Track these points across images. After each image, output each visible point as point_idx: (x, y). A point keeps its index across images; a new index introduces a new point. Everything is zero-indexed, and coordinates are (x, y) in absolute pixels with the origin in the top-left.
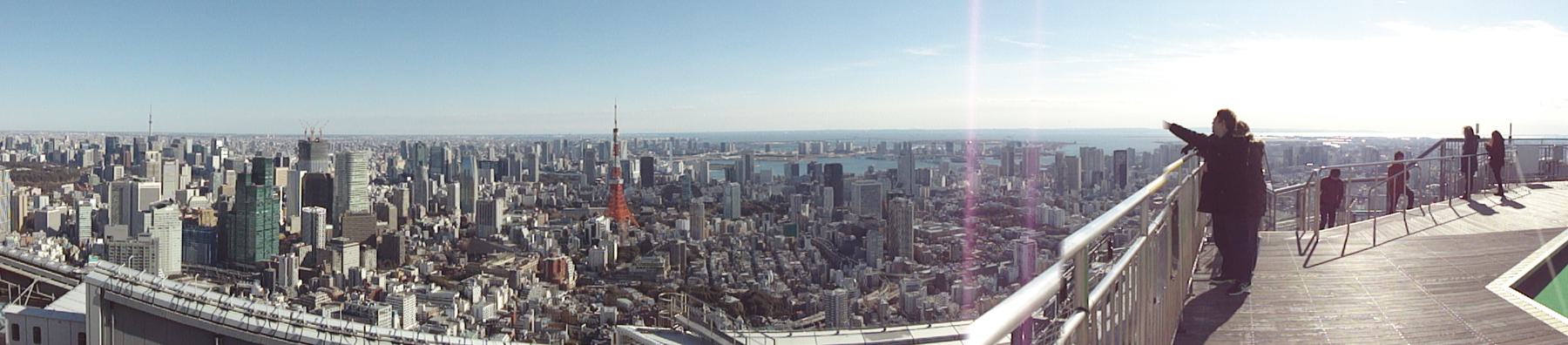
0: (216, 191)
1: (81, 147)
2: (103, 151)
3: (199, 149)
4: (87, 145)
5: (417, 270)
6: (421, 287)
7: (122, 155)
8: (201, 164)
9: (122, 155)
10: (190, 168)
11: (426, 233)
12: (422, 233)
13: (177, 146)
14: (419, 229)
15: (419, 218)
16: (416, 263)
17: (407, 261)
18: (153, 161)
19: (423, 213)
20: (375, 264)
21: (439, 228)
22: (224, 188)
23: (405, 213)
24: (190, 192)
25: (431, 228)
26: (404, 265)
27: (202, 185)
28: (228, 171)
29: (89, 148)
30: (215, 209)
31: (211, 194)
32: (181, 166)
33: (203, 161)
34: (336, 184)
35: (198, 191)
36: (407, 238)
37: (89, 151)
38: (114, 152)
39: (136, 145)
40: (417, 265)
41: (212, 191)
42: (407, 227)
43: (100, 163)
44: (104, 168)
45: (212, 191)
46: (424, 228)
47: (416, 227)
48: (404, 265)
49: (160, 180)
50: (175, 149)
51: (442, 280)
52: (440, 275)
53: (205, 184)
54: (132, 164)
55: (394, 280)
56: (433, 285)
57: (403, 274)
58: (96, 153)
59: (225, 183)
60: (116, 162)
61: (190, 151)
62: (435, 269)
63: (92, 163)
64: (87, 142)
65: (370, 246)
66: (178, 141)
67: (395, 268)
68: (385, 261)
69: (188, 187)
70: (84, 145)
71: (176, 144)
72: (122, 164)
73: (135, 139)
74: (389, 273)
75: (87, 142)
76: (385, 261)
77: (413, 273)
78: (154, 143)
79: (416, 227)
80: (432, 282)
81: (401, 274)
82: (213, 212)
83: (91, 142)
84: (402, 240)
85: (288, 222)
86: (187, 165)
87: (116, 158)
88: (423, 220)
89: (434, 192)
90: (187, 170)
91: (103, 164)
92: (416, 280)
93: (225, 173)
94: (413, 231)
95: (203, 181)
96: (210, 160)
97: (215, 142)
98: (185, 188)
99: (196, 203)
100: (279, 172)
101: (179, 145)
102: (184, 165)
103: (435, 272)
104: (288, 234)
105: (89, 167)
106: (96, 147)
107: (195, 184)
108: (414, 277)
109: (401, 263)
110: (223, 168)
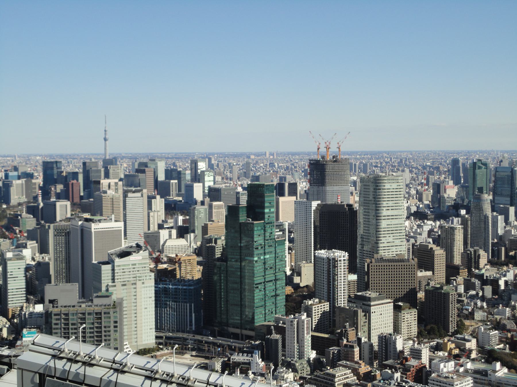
0: (199, 231)
1: (7, 176)
2: (39, 180)
3: (174, 174)
4: (16, 173)
5: (474, 341)
6: (481, 366)
7: (66, 185)
8: (178, 195)
9: (66, 185)
10: (163, 200)
11: (488, 290)
12: (483, 289)
13: (143, 172)
14: (477, 282)
15: (478, 268)
16: (474, 331)
17: (460, 328)
18: (111, 193)
19: (483, 261)
20: (415, 330)
21: (506, 282)
22: (209, 226)
23: (457, 260)
24: (164, 234)
25: (494, 283)
26: (456, 332)
27: (180, 223)
28: (215, 203)
29: (19, 178)
30: (198, 255)
31: (192, 235)
32: (150, 198)
33: (180, 190)
34: (361, 219)
35: (174, 232)
36: (460, 295)
37: (19, 182)
38: (55, 182)
39: (86, 173)
40: (475, 335)
41: (193, 231)
42: (460, 279)
43: (36, 198)
44: (42, 205)
45: (193, 231)
46: (485, 282)
47: (473, 280)
48: (456, 332)
49: (122, 218)
50: (141, 176)
51: (508, 359)
52: (507, 351)
53: (184, 221)
54: (82, 198)
55: (441, 353)
56: (498, 365)
57: (453, 346)
58: (29, 186)
59: (210, 221)
60: (59, 197)
61: (161, 177)
62: (501, 341)
63: (24, 199)
64: (16, 169)
65: (408, 305)
66: (146, 165)
67: (441, 337)
68: (429, 327)
69: (161, 227)
70: (11, 174)
71: (142, 169)
72: (67, 198)
73: (84, 164)
74: (434, 343)
75: (16, 169)
76: (429, 327)
77: (468, 345)
78: (112, 169)
79: (473, 280)
80: (497, 360)
81: (451, 346)
82: (196, 259)
83: (21, 170)
84: (453, 298)
85: (297, 271)
86: (158, 197)
87: (58, 191)
88: (483, 271)
89: (500, 232)
90: (159, 203)
91: (40, 199)
92: (473, 355)
93: (211, 207)
94: (468, 286)
95: (181, 218)
96: (190, 189)
97: (194, 164)
98: (156, 227)
99: (172, 247)
100: (283, 202)
101: (146, 169)
102: (154, 198)
103: (501, 346)
104: (296, 287)
105: (20, 204)
106: (29, 176)
107: (171, 222)
108: (470, 351)
109: (451, 330)
110: (207, 200)
